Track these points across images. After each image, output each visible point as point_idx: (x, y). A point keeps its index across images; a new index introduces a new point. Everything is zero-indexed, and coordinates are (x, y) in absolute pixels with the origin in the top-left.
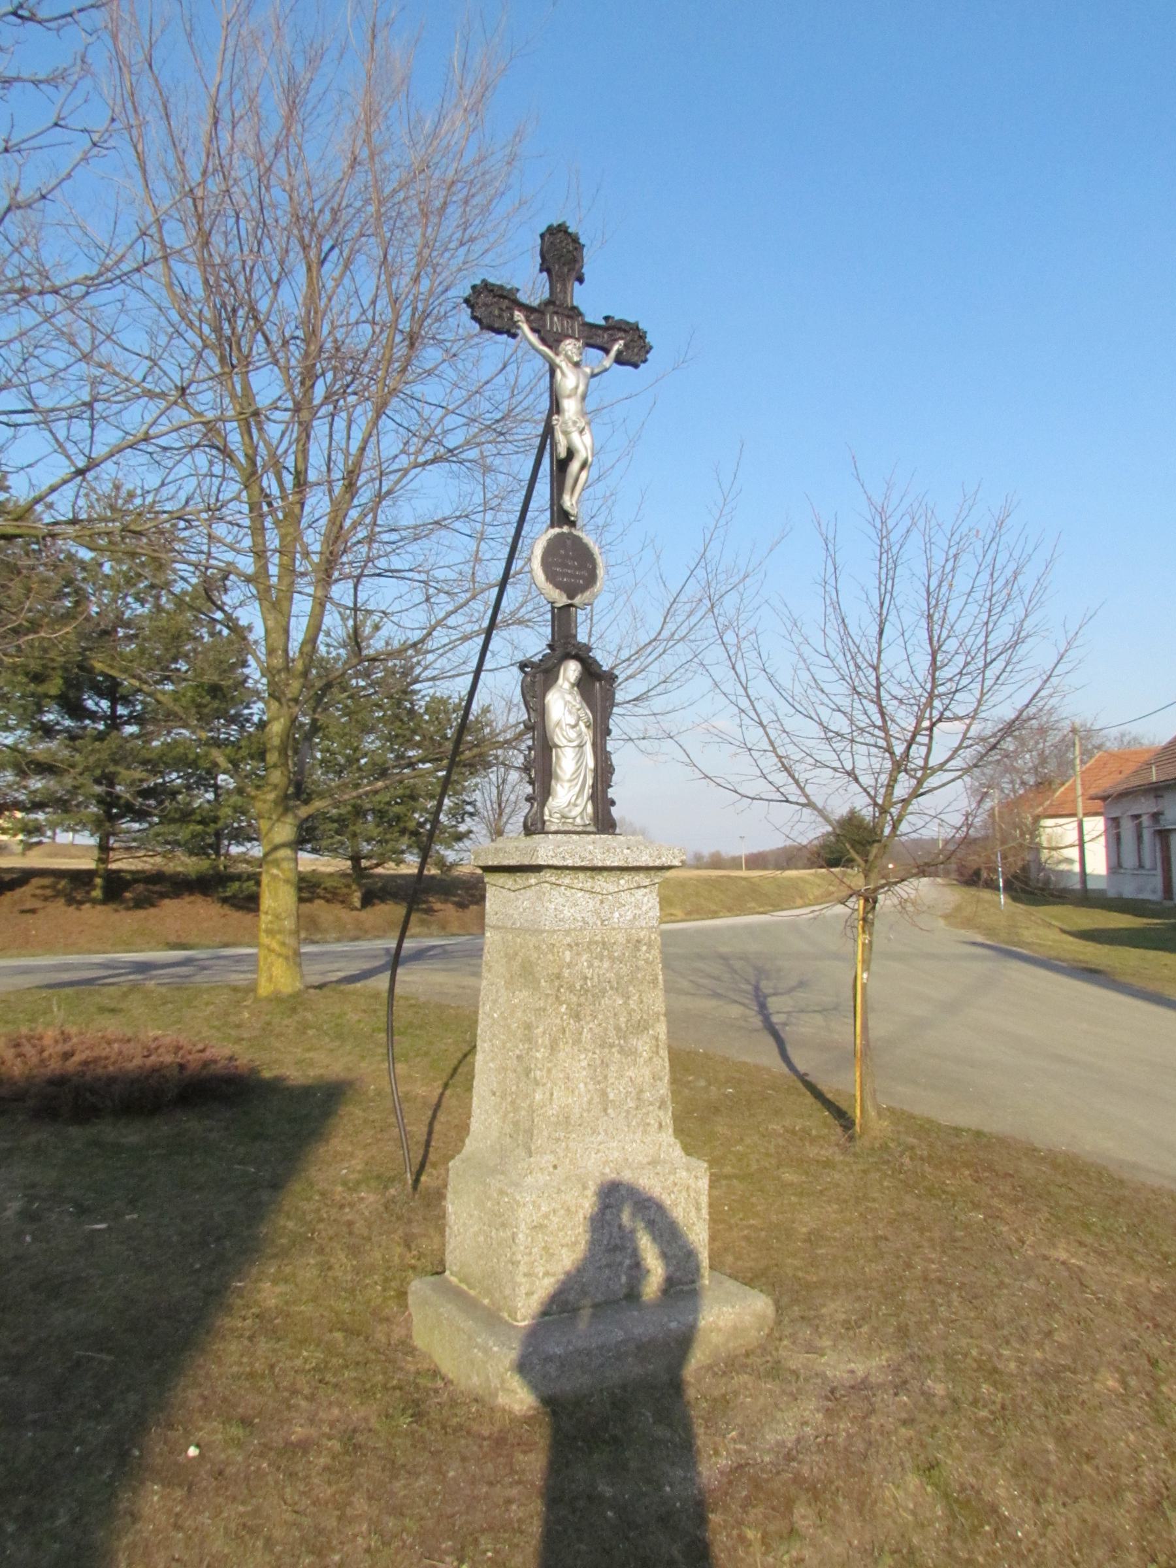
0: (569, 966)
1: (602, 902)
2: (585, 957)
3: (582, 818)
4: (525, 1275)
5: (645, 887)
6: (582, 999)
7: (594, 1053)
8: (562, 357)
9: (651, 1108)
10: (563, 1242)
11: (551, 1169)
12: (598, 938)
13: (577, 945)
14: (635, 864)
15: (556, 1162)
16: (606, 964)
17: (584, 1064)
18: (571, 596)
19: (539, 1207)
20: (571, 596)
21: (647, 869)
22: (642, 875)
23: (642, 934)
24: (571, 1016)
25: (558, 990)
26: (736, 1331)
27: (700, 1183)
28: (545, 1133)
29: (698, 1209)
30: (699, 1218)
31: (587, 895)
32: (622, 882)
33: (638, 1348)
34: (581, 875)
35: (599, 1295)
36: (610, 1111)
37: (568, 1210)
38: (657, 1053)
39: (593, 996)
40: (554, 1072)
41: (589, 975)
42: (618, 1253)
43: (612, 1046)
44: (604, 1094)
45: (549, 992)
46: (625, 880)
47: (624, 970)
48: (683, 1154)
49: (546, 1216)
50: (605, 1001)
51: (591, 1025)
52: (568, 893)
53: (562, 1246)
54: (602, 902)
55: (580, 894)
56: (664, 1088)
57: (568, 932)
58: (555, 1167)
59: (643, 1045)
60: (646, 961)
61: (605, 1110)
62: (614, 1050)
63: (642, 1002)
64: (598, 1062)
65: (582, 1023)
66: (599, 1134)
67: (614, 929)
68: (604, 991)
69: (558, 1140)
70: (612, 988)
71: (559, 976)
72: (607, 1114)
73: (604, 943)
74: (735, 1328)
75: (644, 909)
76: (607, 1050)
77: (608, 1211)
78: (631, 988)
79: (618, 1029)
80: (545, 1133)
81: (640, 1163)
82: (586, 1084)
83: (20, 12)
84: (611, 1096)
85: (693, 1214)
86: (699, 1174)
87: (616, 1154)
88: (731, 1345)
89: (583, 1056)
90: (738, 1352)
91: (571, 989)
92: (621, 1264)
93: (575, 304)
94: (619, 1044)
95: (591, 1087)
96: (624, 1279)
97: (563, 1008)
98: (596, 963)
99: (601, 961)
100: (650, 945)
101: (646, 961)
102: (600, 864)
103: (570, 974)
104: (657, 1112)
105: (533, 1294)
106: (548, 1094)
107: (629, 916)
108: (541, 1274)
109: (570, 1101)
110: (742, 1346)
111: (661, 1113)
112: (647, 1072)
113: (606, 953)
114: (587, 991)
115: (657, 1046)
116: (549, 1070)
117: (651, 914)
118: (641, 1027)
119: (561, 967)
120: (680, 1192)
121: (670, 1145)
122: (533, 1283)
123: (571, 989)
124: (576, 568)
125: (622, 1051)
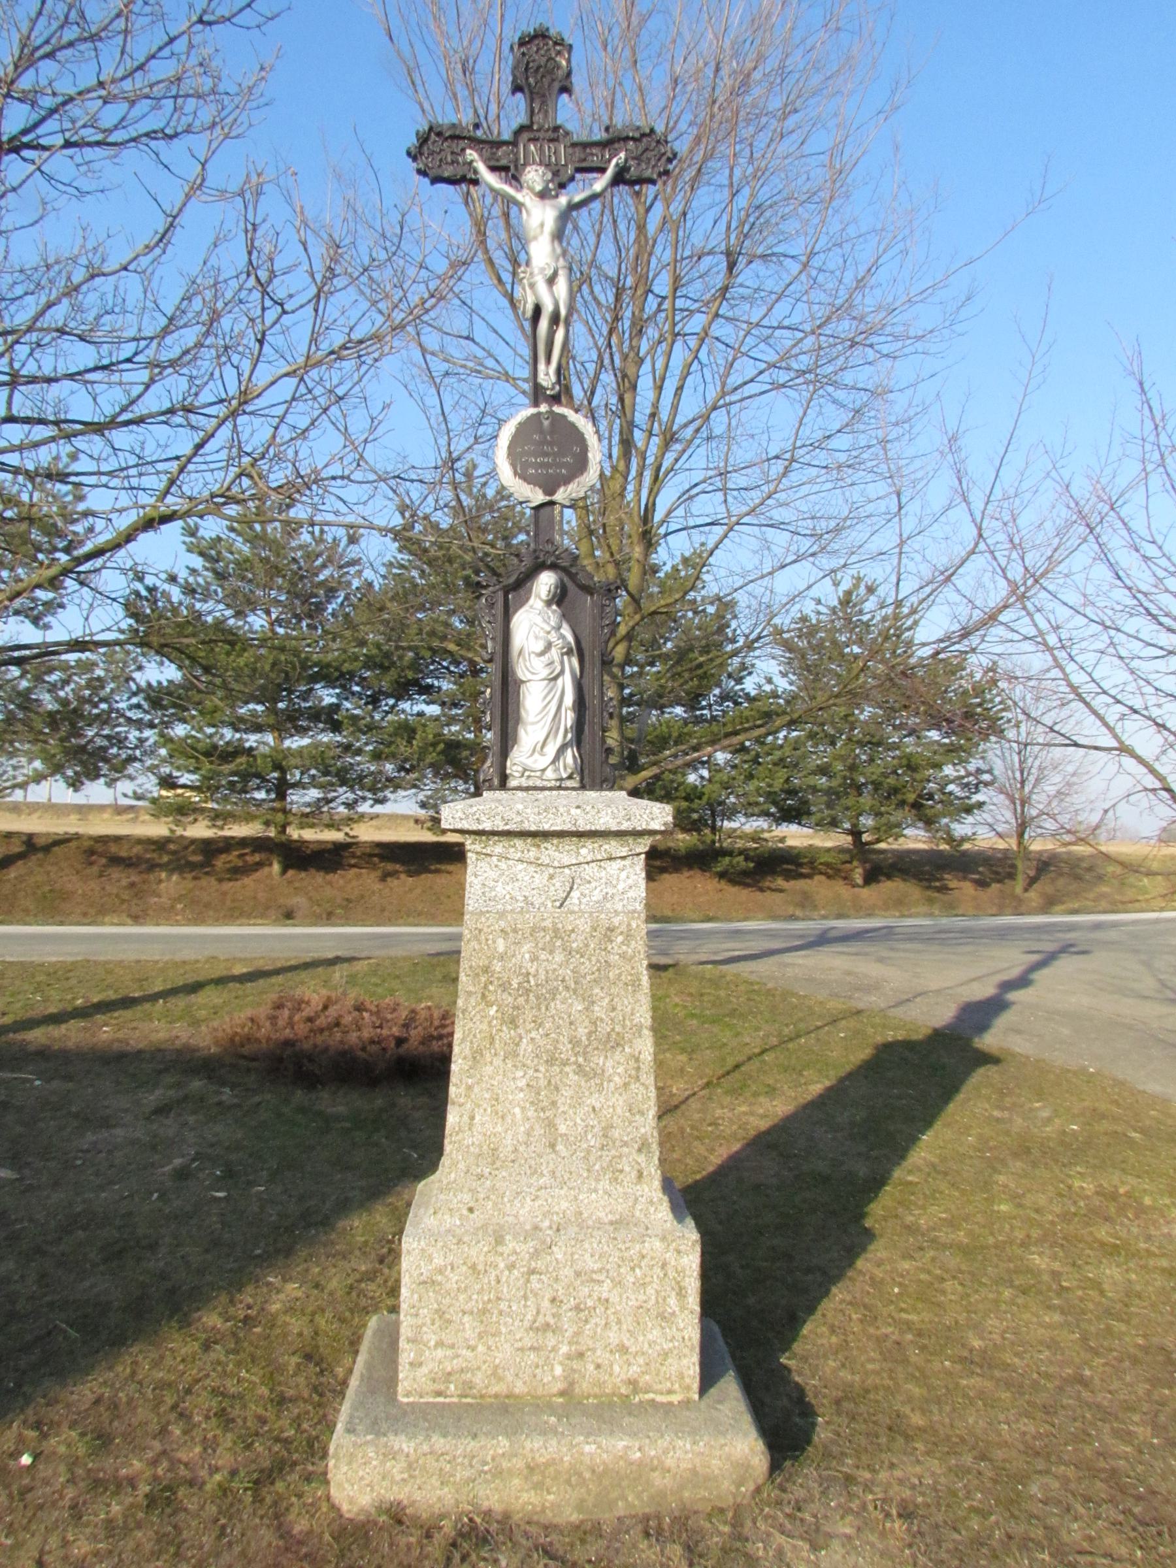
0: (501, 958)
1: (551, 877)
2: (526, 948)
3: (557, 770)
4: (409, 1341)
5: (623, 858)
6: (521, 1000)
7: (537, 1071)
8: (525, 191)
9: (625, 1150)
10: (467, 1308)
11: (465, 1212)
12: (548, 923)
13: (515, 931)
14: (588, 828)
15: (471, 1204)
16: (559, 957)
17: (522, 1083)
18: (550, 491)
19: (430, 1259)
20: (550, 491)
21: (620, 834)
22: (613, 843)
23: (616, 921)
24: (503, 1022)
25: (485, 987)
26: (695, 1477)
27: (685, 1260)
28: (462, 1166)
29: (681, 1293)
30: (683, 1308)
31: (532, 869)
32: (584, 851)
33: (531, 1469)
34: (518, 842)
35: (519, 1384)
36: (559, 1147)
37: (473, 1267)
38: (638, 1078)
39: (538, 998)
40: (476, 1089)
41: (532, 971)
42: (550, 1334)
43: (565, 1063)
44: (551, 1125)
45: (471, 988)
46: (587, 850)
47: (587, 967)
48: (671, 1216)
49: (440, 1271)
50: (557, 1005)
51: (533, 1034)
52: (503, 865)
53: (464, 1313)
54: (551, 877)
55: (521, 866)
56: (647, 1125)
57: (502, 915)
58: (471, 1210)
59: (614, 1065)
60: (623, 956)
61: (552, 1146)
62: (567, 1069)
63: (614, 1009)
64: (543, 1083)
65: (521, 1031)
66: (542, 1175)
67: (572, 912)
68: (554, 993)
69: (480, 1177)
70: (567, 988)
71: (486, 970)
72: (554, 1151)
73: (556, 931)
74: (694, 1471)
75: (621, 886)
76: (557, 1069)
77: (534, 1278)
78: (597, 990)
79: (574, 1042)
80: (462, 1166)
81: (599, 1221)
82: (523, 1109)
83: (206, 18)
84: (562, 1129)
85: (672, 1301)
86: (682, 1248)
87: (564, 1205)
88: (686, 1494)
89: (520, 1074)
90: (699, 1506)
91: (505, 987)
92: (554, 1349)
93: (559, 122)
94: (576, 1063)
95: (530, 1113)
96: (558, 1370)
97: (493, 1011)
98: (543, 956)
99: (551, 952)
100: (629, 936)
101: (623, 956)
102: (533, 828)
103: (504, 968)
104: (635, 1156)
105: (421, 1364)
106: (466, 1118)
107: (597, 896)
108: (432, 1343)
109: (499, 1129)
110: (703, 1499)
111: (641, 1159)
112: (619, 1101)
113: (558, 943)
114: (528, 991)
115: (638, 1069)
116: (470, 1088)
117: (631, 894)
118: (613, 1042)
119: (491, 958)
120: (651, 1267)
121: (651, 1203)
122: (420, 1353)
123: (505, 987)
124: (555, 455)
125: (580, 1070)
